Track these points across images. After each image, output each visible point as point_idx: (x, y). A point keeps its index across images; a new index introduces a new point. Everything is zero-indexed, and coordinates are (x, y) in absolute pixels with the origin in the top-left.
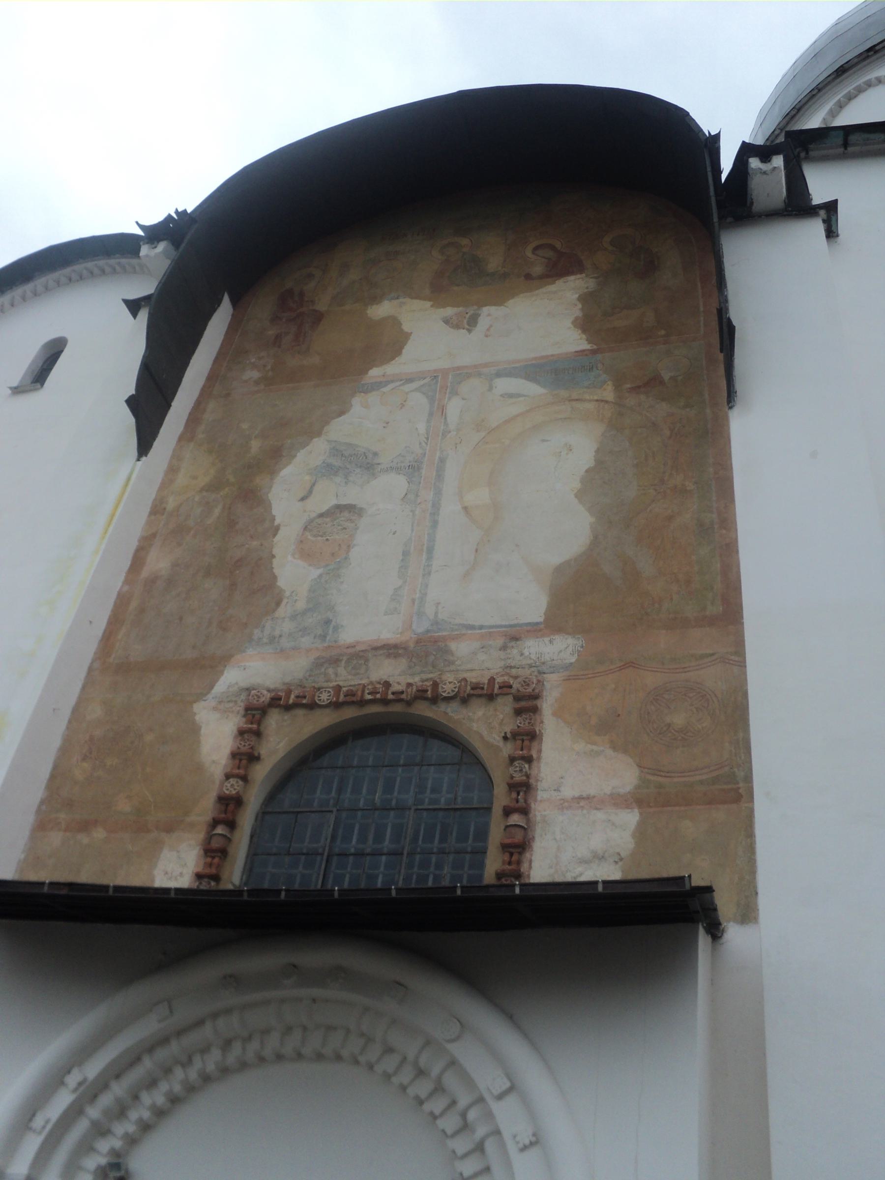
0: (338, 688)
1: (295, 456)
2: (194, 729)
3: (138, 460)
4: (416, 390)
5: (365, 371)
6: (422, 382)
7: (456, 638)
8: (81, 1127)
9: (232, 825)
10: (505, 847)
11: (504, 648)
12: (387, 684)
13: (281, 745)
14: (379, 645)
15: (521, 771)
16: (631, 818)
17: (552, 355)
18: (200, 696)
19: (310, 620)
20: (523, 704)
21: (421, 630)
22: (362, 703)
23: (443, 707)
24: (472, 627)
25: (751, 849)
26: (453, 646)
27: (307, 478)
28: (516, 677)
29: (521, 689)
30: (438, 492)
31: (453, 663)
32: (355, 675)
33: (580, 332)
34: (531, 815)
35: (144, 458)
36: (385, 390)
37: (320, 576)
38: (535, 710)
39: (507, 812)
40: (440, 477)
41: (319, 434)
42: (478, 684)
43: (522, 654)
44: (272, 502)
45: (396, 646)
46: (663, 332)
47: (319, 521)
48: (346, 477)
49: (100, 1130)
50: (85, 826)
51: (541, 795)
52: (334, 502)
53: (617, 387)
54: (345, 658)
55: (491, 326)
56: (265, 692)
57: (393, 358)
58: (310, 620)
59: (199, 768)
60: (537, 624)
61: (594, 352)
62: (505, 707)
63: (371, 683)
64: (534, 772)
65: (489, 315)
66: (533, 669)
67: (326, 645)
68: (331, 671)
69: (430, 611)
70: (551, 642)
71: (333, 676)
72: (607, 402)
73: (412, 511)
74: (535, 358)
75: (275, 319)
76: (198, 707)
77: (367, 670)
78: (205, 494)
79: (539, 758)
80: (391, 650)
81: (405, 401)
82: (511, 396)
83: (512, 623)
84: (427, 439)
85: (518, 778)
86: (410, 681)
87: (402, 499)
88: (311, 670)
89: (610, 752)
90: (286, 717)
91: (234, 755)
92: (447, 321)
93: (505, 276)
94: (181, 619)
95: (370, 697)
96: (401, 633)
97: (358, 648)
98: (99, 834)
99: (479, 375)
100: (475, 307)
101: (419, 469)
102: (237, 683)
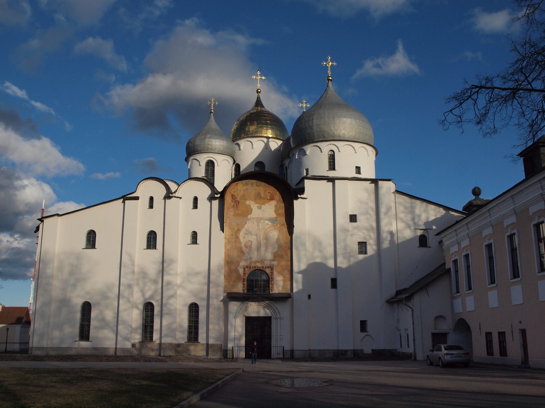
5: (248, 216)
7: (265, 261)
18: (238, 266)
24: (266, 260)
27: (244, 235)
36: (251, 220)
37: (248, 251)
41: (243, 227)
48: (249, 235)
53: (280, 224)
57: (251, 214)
61: (277, 217)
69: (261, 257)
76: (238, 268)
80: (258, 262)
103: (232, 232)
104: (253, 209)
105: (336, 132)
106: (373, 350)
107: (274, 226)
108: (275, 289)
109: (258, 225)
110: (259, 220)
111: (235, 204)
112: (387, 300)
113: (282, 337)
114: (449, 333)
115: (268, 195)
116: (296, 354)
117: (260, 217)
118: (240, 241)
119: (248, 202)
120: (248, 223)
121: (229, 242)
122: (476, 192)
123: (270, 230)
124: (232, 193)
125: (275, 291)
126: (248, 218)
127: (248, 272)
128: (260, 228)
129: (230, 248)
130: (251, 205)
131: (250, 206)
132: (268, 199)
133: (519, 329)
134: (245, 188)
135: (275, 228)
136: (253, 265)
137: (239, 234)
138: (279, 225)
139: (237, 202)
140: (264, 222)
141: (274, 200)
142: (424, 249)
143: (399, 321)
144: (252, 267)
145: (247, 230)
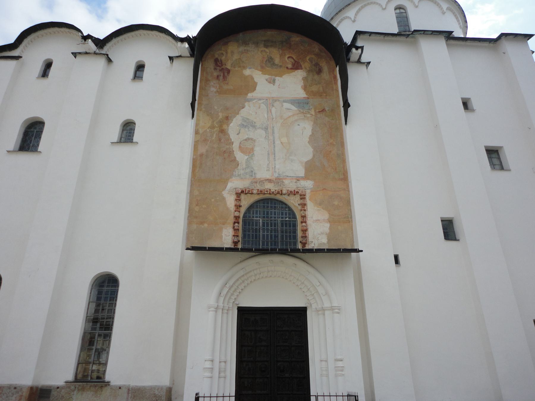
0: (258, 190)
1: (233, 120)
2: (224, 199)
3: (192, 119)
4: (263, 103)
5: (247, 94)
6: (263, 101)
7: (285, 179)
8: (229, 294)
9: (238, 223)
10: (302, 230)
11: (296, 182)
12: (270, 190)
13: (246, 203)
14: (266, 179)
15: (304, 213)
16: (328, 225)
17: (297, 97)
19: (247, 171)
20: (302, 197)
21: (276, 176)
22: (265, 194)
23: (283, 196)
24: (288, 176)
25: (352, 233)
26: (284, 181)
27: (238, 128)
28: (300, 190)
29: (301, 193)
30: (274, 138)
31: (284, 185)
32: (262, 186)
33: (304, 91)
34: (307, 223)
35: (193, 118)
36: (254, 101)
38: (304, 198)
39: (302, 222)
40: (273, 133)
41: (238, 114)
42: (291, 191)
43: (300, 184)
44: (230, 134)
45: (270, 180)
46: (325, 95)
47: (244, 141)
48: (248, 128)
49: (232, 294)
50: (202, 223)
51: (308, 219)
52: (247, 137)
53: (315, 111)
54: (258, 182)
55: (280, 85)
56: (240, 189)
57: (254, 91)
58: (247, 171)
59: (228, 209)
60: (303, 177)
61: (308, 98)
62: (298, 197)
63: (266, 189)
64: (306, 213)
65: (278, 80)
66: (303, 189)
67: (253, 178)
68: (255, 185)
70: (307, 182)
71: (256, 186)
72: (313, 115)
73: (268, 142)
74: (292, 98)
75: (215, 69)
76: (223, 193)
77: (264, 185)
78: (210, 129)
79: (307, 210)
80: (270, 181)
81: (260, 106)
82: (288, 109)
83: (297, 176)
84: (268, 120)
85: (303, 215)
86: (275, 189)
87: (265, 138)
88: (250, 184)
89: (322, 210)
90: (246, 196)
91: (235, 206)
92: (267, 80)
93: (281, 66)
94: (213, 167)
95: (266, 193)
96: (271, 177)
97: (261, 179)
98: (206, 225)
99: (279, 101)
100: (274, 76)
101: (268, 129)
102: (232, 187)
103: (213, 122)
108: (312, 242)
109: (269, 111)
110: (271, 102)
111: (222, 75)
113: (340, 364)
115: (288, 61)
117: (273, 98)
119: (247, 72)
123: (296, 120)
124: (216, 56)
126: (248, 98)
127: (246, 202)
128: (274, 117)
129: (207, 151)
130: (254, 77)
131: (252, 78)
132: (289, 68)
134: (242, 49)
135: (305, 116)
136: (259, 187)
137: (228, 125)
138: (313, 113)
140: (282, 106)
141: (302, 69)
144: (255, 192)
145: (245, 120)
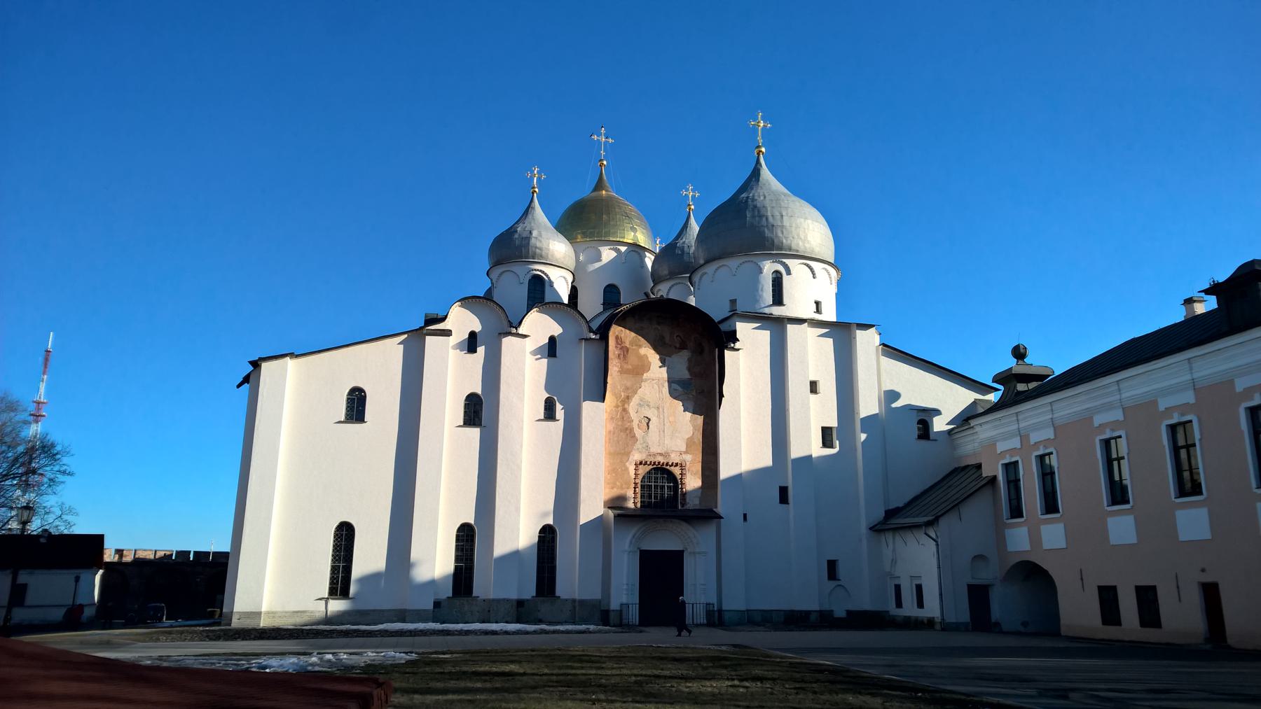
27: (637, 407)
82: (676, 390)
93: (670, 346)
104: (652, 364)
105: (784, 241)
106: (849, 612)
107: (686, 393)
112: (872, 526)
114: (993, 585)
115: (676, 340)
116: (726, 617)
118: (629, 417)
120: (643, 387)
121: (612, 418)
122: (1019, 353)
124: (617, 333)
125: (689, 505)
126: (644, 377)
127: (643, 470)
133: (1199, 582)
139: (625, 350)
142: (923, 443)
143: (896, 562)
